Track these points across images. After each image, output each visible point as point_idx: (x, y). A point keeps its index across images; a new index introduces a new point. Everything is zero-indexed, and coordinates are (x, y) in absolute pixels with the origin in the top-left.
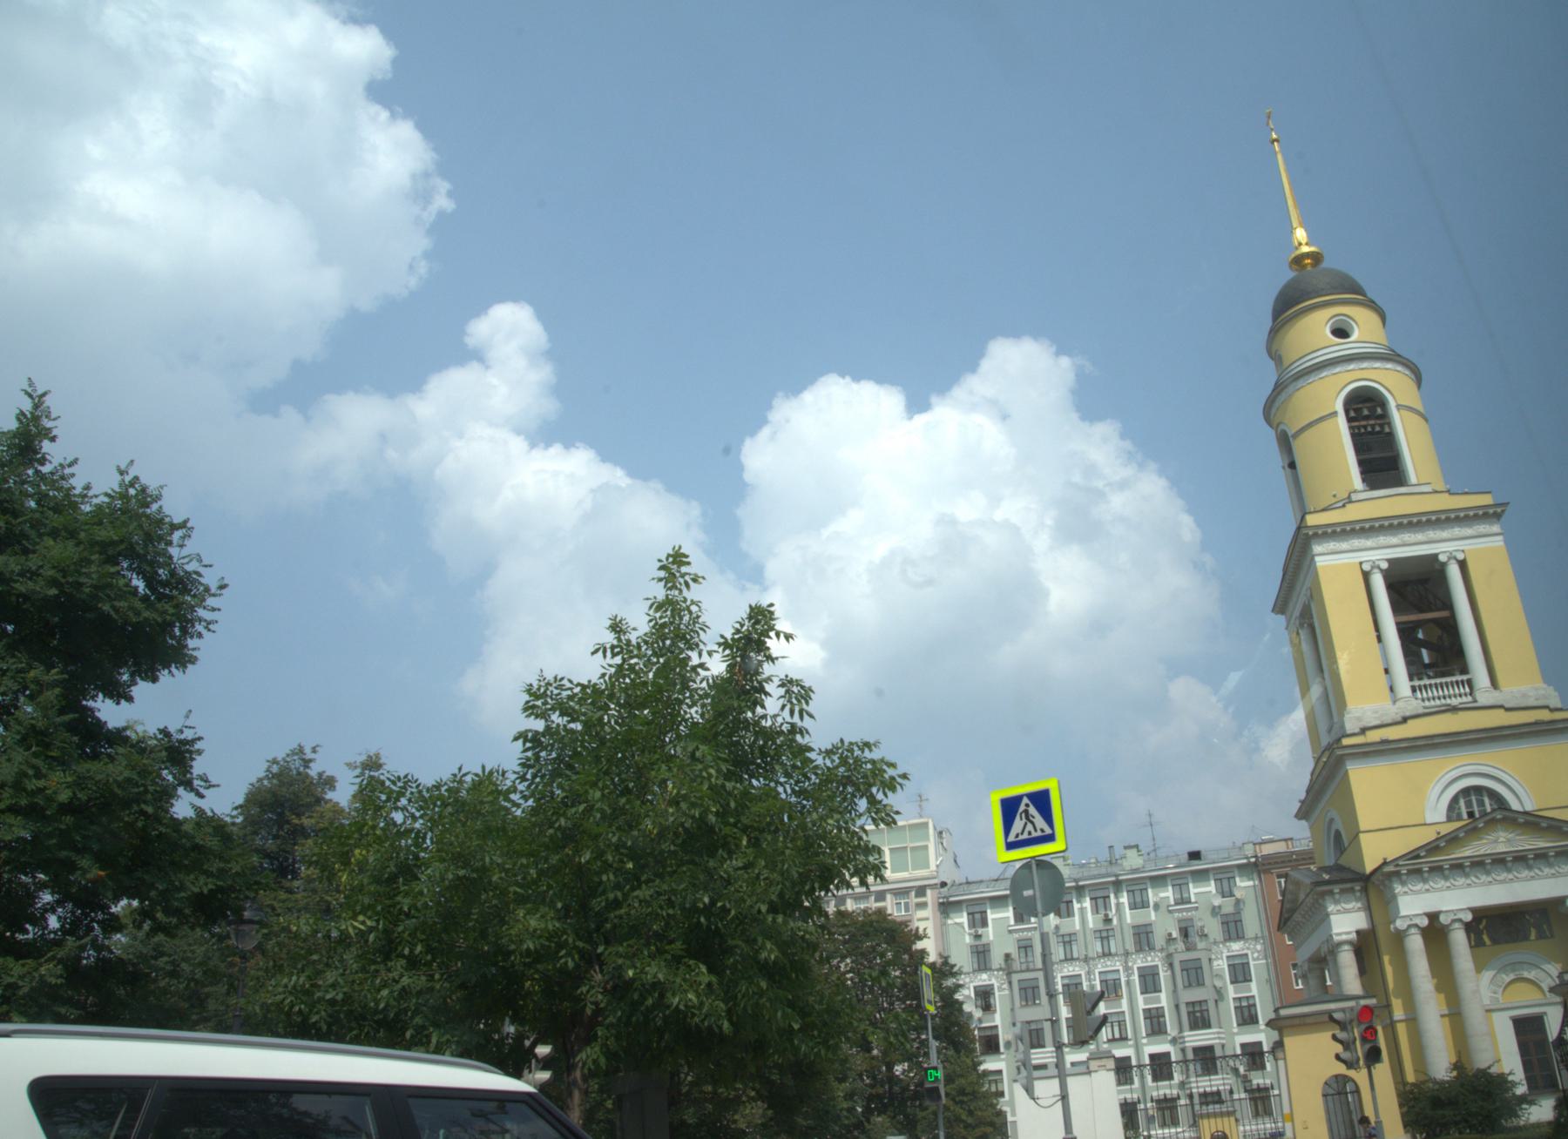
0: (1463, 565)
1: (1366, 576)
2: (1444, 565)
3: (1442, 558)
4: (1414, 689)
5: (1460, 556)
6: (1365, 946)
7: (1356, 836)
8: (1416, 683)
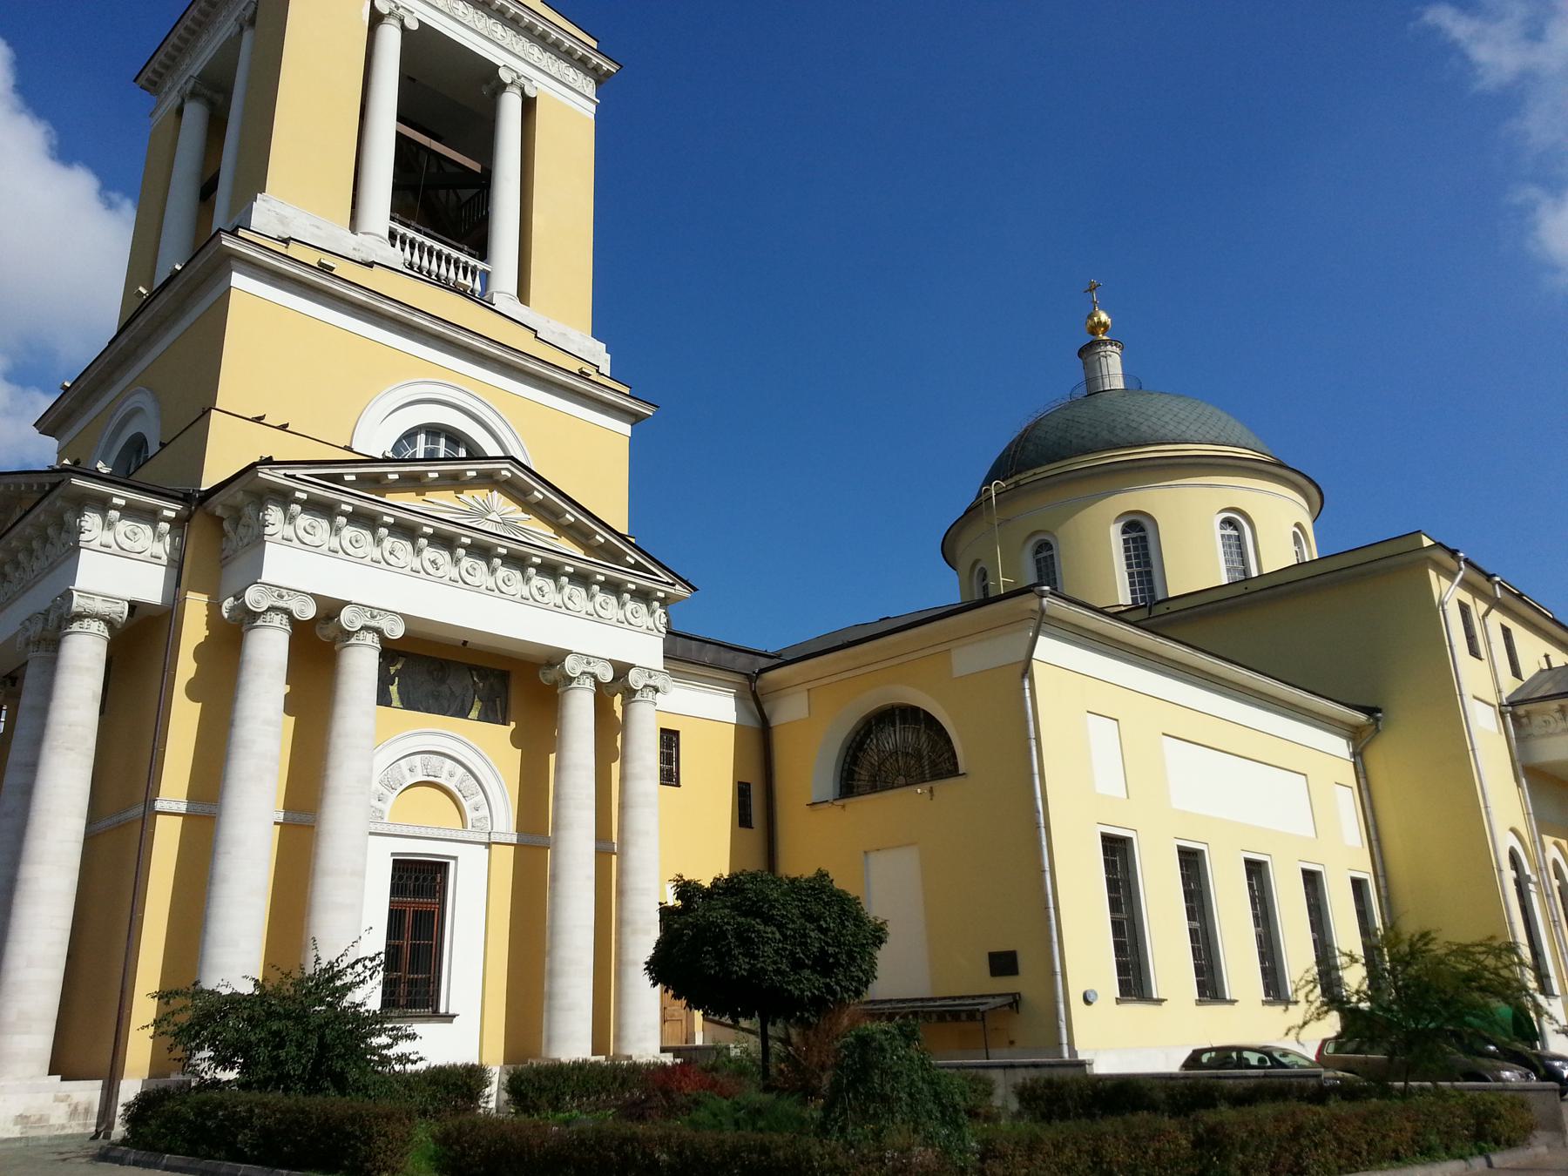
0: (529, 105)
1: (376, 19)
2: (503, 87)
3: (505, 76)
4: (392, 235)
5: (531, 93)
6: (139, 639)
7: (206, 413)
8: (401, 230)
